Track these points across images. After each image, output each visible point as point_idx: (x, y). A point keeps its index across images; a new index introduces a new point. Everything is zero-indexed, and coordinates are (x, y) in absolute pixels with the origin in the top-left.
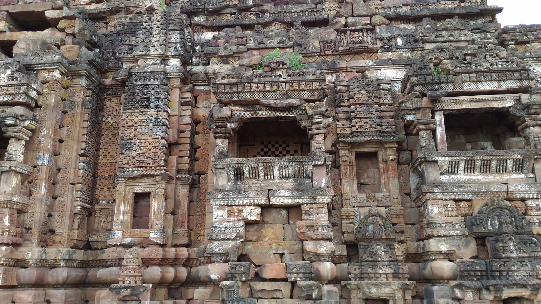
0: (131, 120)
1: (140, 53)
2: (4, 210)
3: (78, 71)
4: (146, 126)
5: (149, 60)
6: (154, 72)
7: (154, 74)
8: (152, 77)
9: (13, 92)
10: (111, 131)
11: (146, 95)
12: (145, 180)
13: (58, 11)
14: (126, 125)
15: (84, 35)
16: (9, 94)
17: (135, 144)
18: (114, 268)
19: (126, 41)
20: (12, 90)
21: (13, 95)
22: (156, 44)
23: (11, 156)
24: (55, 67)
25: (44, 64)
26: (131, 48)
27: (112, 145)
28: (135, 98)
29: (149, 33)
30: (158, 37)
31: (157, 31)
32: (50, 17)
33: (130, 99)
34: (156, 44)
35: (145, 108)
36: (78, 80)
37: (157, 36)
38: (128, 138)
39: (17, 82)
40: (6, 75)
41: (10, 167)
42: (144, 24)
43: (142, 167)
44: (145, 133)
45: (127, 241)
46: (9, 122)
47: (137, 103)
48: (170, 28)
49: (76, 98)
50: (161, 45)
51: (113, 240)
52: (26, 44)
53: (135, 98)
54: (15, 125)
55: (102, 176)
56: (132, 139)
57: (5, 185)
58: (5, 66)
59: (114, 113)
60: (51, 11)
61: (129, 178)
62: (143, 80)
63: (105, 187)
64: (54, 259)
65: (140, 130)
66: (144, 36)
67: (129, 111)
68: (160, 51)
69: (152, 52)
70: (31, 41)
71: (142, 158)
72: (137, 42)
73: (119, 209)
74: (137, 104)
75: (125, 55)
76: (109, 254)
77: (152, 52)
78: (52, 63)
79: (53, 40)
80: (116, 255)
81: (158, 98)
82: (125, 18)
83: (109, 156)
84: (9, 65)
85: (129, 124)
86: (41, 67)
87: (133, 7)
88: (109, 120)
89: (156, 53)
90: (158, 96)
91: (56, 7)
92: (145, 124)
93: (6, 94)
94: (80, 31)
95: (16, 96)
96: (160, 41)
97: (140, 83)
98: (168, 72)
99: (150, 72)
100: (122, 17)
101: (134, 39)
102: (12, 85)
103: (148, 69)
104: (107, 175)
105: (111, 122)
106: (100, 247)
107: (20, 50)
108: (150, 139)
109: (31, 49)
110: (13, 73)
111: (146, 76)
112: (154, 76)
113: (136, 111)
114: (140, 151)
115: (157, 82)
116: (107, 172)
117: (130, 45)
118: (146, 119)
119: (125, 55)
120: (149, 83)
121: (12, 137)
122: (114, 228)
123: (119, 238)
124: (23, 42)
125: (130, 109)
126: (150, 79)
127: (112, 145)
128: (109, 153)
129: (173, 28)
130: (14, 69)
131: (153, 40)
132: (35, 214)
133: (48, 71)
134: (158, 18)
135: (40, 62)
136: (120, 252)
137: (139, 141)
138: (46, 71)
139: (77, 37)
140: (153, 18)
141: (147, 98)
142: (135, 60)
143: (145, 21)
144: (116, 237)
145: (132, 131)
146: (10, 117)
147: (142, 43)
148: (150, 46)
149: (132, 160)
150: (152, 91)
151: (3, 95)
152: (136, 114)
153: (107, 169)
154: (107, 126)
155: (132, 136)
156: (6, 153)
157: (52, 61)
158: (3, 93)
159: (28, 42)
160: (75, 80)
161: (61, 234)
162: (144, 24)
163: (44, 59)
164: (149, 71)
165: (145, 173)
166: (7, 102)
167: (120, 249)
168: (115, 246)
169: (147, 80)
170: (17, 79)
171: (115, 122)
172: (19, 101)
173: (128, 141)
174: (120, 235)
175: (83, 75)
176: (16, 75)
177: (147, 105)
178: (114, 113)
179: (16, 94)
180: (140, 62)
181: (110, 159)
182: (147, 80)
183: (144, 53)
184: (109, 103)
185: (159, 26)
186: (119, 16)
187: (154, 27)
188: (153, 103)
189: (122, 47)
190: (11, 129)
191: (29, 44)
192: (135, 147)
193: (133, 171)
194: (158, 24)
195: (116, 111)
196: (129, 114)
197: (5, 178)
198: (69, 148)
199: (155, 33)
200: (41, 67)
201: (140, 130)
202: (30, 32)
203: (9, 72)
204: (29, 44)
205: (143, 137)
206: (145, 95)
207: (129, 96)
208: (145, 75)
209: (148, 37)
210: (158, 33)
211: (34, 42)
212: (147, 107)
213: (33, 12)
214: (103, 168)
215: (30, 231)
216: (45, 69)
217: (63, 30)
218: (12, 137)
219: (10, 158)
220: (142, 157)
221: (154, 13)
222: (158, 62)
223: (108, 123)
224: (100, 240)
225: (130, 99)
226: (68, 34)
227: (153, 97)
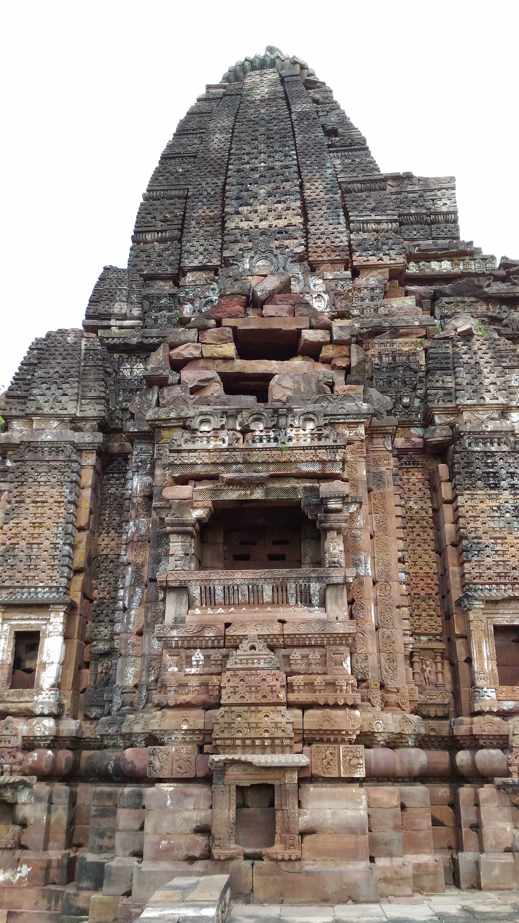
0: (473, 507)
1: (469, 402)
2: (342, 648)
3: (384, 427)
4: (499, 517)
5: (480, 412)
6: (497, 431)
7: (498, 435)
8: (496, 440)
9: (325, 458)
10: (417, 523)
11: (492, 467)
12: (513, 605)
13: (322, 331)
14: (467, 515)
15: (364, 370)
16: (318, 461)
17: (487, 546)
18: (493, 751)
19: (437, 381)
20: (323, 455)
21: (323, 462)
22: (491, 388)
23: (336, 560)
24: (362, 420)
25: (346, 415)
26: (450, 394)
27: (422, 545)
28: (473, 472)
29: (476, 371)
30: (492, 378)
31: (489, 368)
32: (311, 340)
33: (466, 473)
34: (491, 388)
35: (491, 488)
36: (381, 441)
37: (489, 377)
38: (473, 535)
39: (329, 442)
40: (307, 432)
41: (345, 577)
42: (463, 356)
43: (505, 584)
44: (501, 528)
45: (508, 705)
46: (333, 505)
47: (479, 479)
48: (504, 364)
49: (383, 469)
50: (500, 390)
51: (485, 703)
52: (294, 382)
53: (473, 472)
54: (338, 511)
55: (415, 594)
56: (481, 538)
57: (334, 607)
58: (306, 416)
59: (418, 493)
60: (311, 331)
61: (487, 602)
62: (481, 444)
63: (424, 614)
64: (400, 733)
65: (492, 524)
66: (469, 376)
67: (468, 492)
68: (502, 400)
69: (488, 400)
70: (300, 377)
71: (501, 569)
72: (457, 384)
73: (480, 652)
74: (479, 482)
75: (441, 404)
76: (482, 726)
77: (488, 400)
78: (359, 415)
79: (322, 376)
80: (496, 728)
81: (511, 473)
82: (393, 344)
83: (420, 562)
84: (311, 416)
85: (470, 513)
86: (339, 419)
87: (402, 327)
88: (411, 504)
89: (495, 402)
90: (512, 470)
91: (318, 325)
92: (498, 515)
93: (313, 461)
94: (359, 363)
95: (329, 464)
96: (498, 383)
97: (478, 449)
98: (516, 432)
99: (489, 432)
100: (388, 342)
101: (448, 379)
102: (320, 447)
103: (487, 427)
104: (423, 593)
105: (415, 507)
106: (432, 714)
107: (284, 390)
108: (510, 539)
109: (303, 390)
110: (319, 428)
111: (486, 438)
112: (499, 439)
113: (480, 492)
114: (497, 559)
115: (505, 448)
116: (423, 589)
117: (445, 388)
118: (499, 508)
119: (441, 404)
120: (493, 449)
121: (332, 529)
122: (479, 683)
123: (492, 699)
124: (288, 378)
125: (468, 489)
126: (492, 443)
127: (422, 545)
128: (420, 557)
129: (510, 364)
130: (322, 423)
131: (487, 382)
132: (368, 655)
133: (349, 425)
134: (484, 347)
135: (340, 411)
136: (499, 723)
137: (492, 541)
138: (346, 426)
139: (353, 372)
140: (475, 348)
141: (494, 473)
142: (457, 411)
143: (463, 351)
144: (488, 698)
145: (479, 524)
146: (335, 497)
147: (469, 387)
148: (483, 391)
149: (486, 571)
150: (501, 462)
151: (307, 461)
152: (481, 497)
153: (422, 583)
154: (409, 514)
155: (480, 533)
156: (327, 555)
157: (359, 410)
158: (307, 458)
159: (296, 378)
160: (375, 441)
161: (395, 690)
162: (463, 356)
163: (346, 407)
164: (489, 430)
165: (510, 593)
166: (314, 473)
167: (498, 719)
168: (490, 713)
169: (488, 444)
170: (327, 437)
171: (422, 508)
172: (335, 472)
173: (475, 541)
174: (493, 695)
175: (389, 433)
176: (325, 432)
177: (495, 484)
178: (418, 493)
179: (330, 461)
180: (466, 416)
181: (425, 568)
182: (488, 444)
183: (475, 402)
184: (405, 477)
185: (490, 360)
186: (382, 341)
187: (482, 361)
188: (504, 480)
189: (433, 391)
190: (333, 516)
191: (298, 382)
192: (488, 551)
193: (490, 590)
194: (487, 357)
195: (420, 490)
196: (470, 497)
197: (333, 595)
198: (385, 549)
199: (485, 371)
200: (339, 419)
201: (492, 524)
202: (274, 362)
203: (310, 426)
204: (298, 382)
205: (498, 535)
206: (489, 467)
207: (463, 468)
208: (481, 437)
209: (476, 377)
210: (491, 372)
211: (306, 377)
212: (496, 486)
213: (280, 329)
214: (414, 581)
215: (364, 684)
216: (343, 423)
217: (328, 361)
218: (332, 529)
219: (334, 562)
220: (501, 568)
221: (474, 340)
222: (496, 416)
223: (411, 508)
224: (431, 702)
225: (466, 473)
226: (340, 368)
227: (503, 471)
